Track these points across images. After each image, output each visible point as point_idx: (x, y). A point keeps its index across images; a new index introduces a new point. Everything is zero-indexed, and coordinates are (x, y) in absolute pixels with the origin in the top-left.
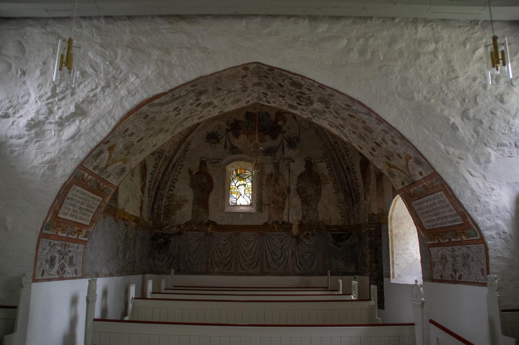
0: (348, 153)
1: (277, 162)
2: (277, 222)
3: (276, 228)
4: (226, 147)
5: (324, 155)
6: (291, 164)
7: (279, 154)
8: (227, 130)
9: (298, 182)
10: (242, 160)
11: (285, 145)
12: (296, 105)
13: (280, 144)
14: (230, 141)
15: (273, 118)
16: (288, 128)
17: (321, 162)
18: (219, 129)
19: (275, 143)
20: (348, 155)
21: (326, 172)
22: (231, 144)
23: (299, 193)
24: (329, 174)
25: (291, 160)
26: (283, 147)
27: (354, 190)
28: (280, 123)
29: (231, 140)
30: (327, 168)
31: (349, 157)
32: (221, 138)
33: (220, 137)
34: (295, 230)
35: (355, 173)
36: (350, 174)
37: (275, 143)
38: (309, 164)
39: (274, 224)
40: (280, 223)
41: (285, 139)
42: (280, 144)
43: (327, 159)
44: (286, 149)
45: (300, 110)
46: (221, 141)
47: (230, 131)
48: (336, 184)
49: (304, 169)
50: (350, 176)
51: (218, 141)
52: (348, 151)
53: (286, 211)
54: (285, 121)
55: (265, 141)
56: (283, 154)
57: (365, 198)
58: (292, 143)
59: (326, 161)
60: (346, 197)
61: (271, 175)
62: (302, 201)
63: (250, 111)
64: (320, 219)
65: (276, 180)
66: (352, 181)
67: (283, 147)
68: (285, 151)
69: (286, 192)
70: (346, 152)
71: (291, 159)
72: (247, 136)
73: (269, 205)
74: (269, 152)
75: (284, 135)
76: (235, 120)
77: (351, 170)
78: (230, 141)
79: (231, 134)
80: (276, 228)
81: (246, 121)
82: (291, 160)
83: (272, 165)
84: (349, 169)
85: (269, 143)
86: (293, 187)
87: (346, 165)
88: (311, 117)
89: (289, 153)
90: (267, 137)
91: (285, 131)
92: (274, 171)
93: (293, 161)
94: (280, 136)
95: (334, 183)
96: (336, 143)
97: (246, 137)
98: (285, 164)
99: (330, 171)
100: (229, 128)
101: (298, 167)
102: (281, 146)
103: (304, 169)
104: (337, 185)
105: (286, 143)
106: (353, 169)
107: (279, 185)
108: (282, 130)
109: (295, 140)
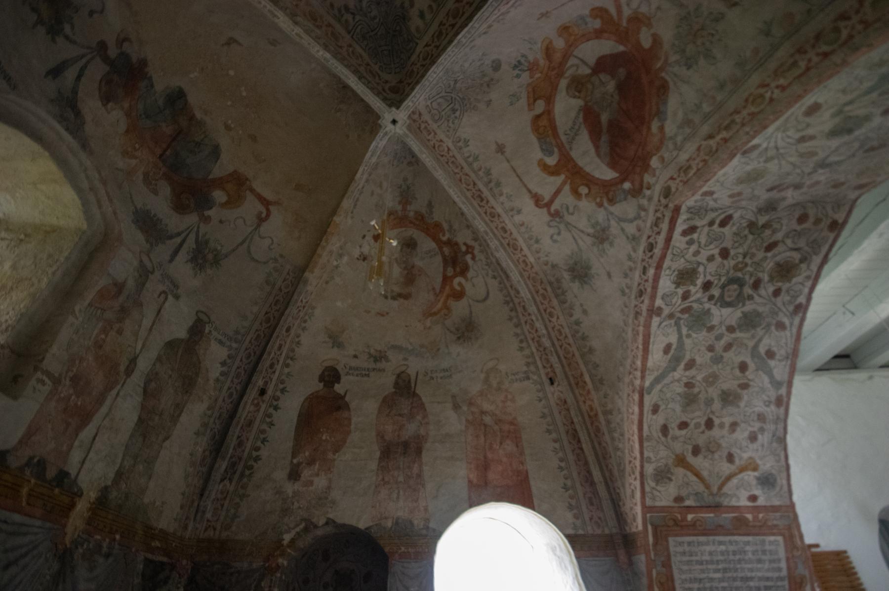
0: (289, 361)
1: (148, 264)
2: (41, 465)
3: (25, 491)
4: (56, 72)
5: (237, 332)
6: (170, 297)
7: (163, 251)
8: (102, 46)
9: (159, 359)
10: (62, 163)
11: (185, 246)
12: (699, 282)
13: (179, 234)
14: (79, 77)
15: (217, 172)
16: (221, 222)
17: (221, 342)
18: (91, 13)
19: (173, 221)
20: (287, 366)
21: (215, 371)
22: (75, 92)
23: (145, 391)
24: (217, 380)
25: (174, 289)
26: (181, 245)
27: (240, 444)
28: (219, 196)
29: (83, 79)
30: (223, 364)
31: (286, 370)
32: (67, 37)
33: (67, 29)
34: (76, 521)
35: (276, 408)
36: (257, 405)
37: (173, 221)
38: (197, 330)
39: (28, 472)
40: (51, 473)
41: (198, 231)
42: (179, 234)
43: (234, 345)
44: (182, 256)
45: (680, 291)
46: (60, 40)
47: (106, 59)
48: (209, 412)
49: (182, 334)
50: (252, 408)
51: (54, 30)
52: (292, 359)
53: (87, 433)
54: (233, 202)
55: (155, 192)
56: (171, 261)
57: (294, 475)
58: (203, 257)
59: (230, 348)
60: (207, 453)
61: (119, 287)
62: (140, 418)
63: (192, 99)
64: (146, 500)
65: (124, 312)
66: (250, 423)
67: (181, 245)
68: (178, 258)
69: (122, 368)
70: (287, 357)
71: (176, 286)
72: (127, 131)
73: (57, 381)
74: (147, 223)
75: (202, 225)
76: (144, 63)
77: (266, 397)
78: (79, 77)
79: (98, 70)
80: (25, 491)
81: (161, 102)
82: (174, 289)
83: (136, 263)
84: (263, 392)
85: (160, 203)
86: (143, 365)
87: (266, 383)
88: (666, 311)
89: (181, 268)
90: (166, 190)
91: (207, 220)
92: (131, 283)
93: (177, 297)
94: (192, 219)
95: (209, 409)
96: (288, 330)
97: (123, 126)
98: (161, 288)
99: (223, 374)
100: (113, 52)
101: (177, 322)
102: (178, 240)
103: (182, 334)
104: (210, 417)
105: (191, 243)
106: (277, 399)
107: (120, 332)
108: (207, 213)
109: (210, 257)
